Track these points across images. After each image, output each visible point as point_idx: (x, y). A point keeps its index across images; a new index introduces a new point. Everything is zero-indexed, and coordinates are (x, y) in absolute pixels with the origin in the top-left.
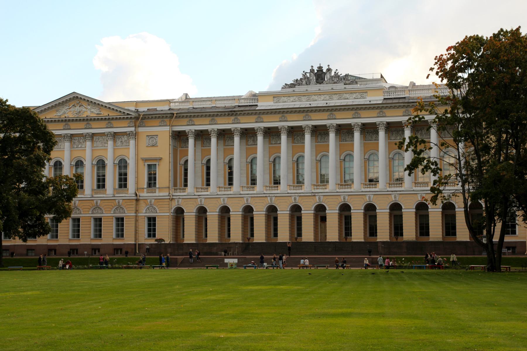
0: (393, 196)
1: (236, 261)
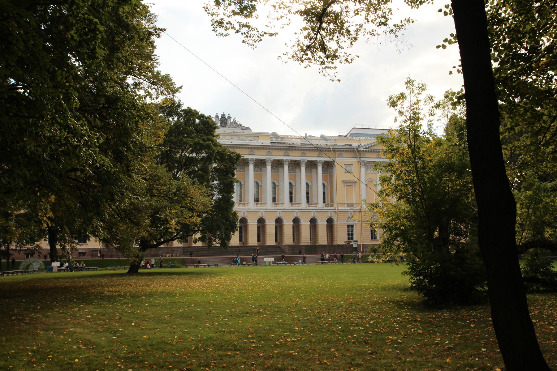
0: (278, 213)
1: (273, 259)
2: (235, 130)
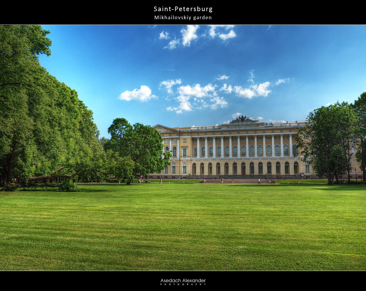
2: (248, 123)
